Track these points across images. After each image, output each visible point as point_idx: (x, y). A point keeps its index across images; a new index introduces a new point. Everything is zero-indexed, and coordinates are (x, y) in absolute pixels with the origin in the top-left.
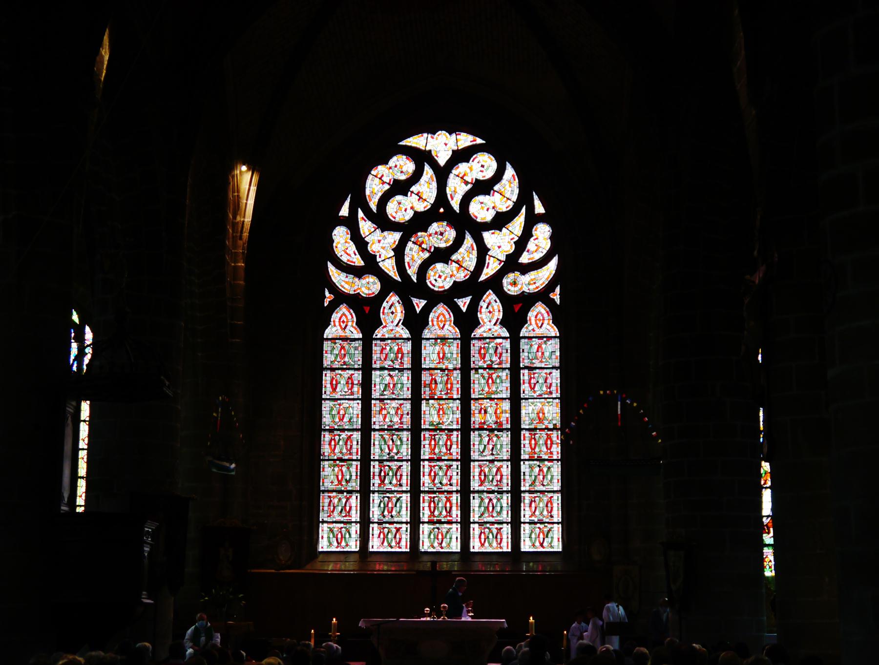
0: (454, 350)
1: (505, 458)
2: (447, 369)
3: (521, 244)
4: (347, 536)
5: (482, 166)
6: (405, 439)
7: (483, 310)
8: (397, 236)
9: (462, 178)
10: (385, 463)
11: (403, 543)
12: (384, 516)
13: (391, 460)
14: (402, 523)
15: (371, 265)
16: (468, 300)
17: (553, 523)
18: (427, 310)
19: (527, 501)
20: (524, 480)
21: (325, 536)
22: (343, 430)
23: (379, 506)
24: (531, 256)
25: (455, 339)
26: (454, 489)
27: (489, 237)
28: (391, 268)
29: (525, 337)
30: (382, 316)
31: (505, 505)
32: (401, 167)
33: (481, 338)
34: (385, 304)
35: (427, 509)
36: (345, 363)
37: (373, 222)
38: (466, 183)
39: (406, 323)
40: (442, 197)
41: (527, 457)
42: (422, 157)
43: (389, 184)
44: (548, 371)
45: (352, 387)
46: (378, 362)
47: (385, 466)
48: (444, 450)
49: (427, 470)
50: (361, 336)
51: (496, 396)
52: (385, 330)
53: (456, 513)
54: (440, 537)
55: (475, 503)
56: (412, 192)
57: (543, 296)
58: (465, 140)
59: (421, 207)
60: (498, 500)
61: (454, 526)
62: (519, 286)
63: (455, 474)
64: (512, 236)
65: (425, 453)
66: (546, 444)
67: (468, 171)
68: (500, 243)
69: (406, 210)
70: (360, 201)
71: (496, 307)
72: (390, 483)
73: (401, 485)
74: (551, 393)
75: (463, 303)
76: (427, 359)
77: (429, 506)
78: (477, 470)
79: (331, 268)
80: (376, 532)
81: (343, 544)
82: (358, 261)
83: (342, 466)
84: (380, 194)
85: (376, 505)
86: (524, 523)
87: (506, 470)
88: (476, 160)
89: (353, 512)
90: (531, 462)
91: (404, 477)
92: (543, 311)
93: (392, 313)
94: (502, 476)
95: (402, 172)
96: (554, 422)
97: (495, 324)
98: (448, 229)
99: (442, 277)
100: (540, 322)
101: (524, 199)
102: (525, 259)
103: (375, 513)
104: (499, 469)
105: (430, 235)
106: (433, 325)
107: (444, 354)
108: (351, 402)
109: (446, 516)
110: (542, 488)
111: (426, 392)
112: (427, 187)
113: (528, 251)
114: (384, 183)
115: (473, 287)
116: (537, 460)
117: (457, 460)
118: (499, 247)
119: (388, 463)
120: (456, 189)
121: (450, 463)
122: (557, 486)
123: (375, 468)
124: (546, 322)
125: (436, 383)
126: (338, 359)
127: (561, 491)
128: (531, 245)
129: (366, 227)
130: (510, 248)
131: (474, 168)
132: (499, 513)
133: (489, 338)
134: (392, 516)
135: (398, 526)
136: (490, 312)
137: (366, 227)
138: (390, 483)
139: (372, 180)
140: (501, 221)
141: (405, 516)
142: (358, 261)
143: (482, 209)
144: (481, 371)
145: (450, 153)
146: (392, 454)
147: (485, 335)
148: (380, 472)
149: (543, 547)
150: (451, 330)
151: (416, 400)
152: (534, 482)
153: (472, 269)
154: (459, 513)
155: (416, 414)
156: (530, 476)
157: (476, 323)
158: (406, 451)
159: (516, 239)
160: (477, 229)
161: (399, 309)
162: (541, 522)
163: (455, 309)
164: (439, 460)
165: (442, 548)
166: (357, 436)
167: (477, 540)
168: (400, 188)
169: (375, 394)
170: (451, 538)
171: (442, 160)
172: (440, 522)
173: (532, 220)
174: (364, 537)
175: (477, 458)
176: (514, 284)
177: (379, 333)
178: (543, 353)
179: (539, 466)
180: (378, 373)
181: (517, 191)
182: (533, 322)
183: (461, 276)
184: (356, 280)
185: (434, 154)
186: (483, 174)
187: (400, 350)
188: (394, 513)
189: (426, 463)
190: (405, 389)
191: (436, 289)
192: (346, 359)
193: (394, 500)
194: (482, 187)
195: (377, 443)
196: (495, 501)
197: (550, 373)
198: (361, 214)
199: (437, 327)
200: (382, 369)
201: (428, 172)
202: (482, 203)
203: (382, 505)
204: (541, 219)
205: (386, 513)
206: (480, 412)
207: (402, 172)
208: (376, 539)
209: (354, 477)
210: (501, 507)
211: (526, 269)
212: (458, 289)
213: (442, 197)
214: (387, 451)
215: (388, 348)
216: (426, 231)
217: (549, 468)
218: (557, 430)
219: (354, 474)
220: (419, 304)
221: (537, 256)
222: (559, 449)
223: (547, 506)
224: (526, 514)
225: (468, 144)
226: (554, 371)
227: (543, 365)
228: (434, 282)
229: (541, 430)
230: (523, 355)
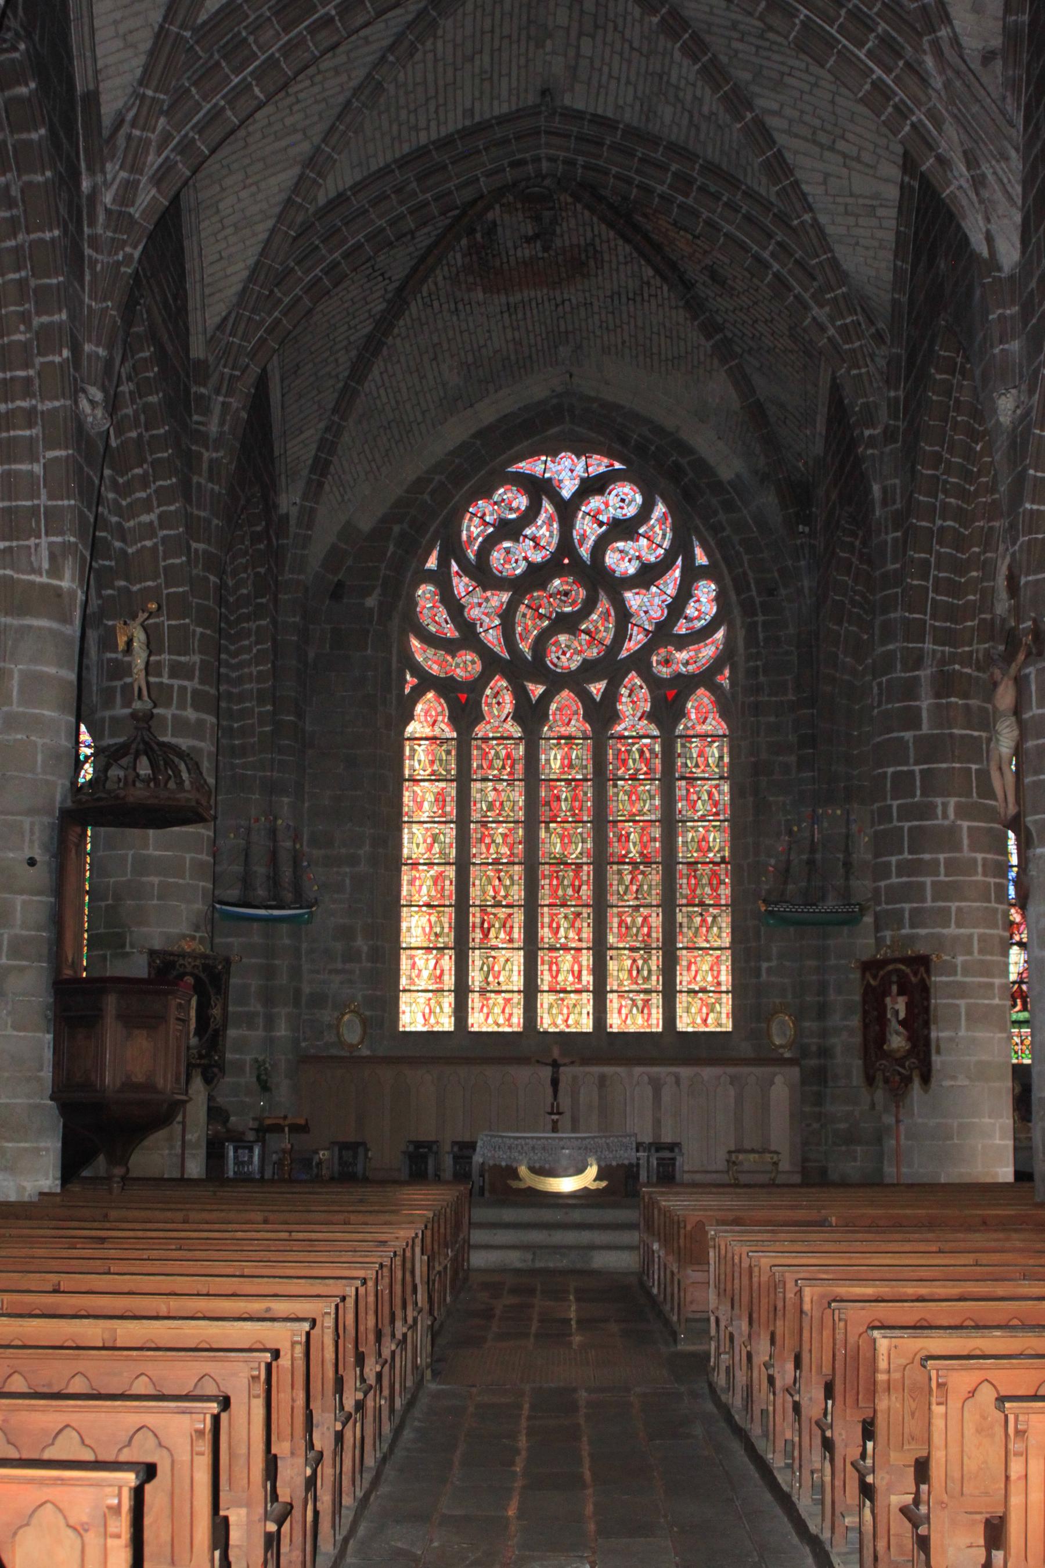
0: (581, 753)
1: (654, 903)
2: (574, 780)
3: (677, 607)
4: (438, 1010)
5: (623, 500)
6: (516, 878)
7: (624, 700)
8: (505, 597)
9: (594, 516)
10: (489, 910)
11: (515, 1020)
12: (488, 984)
14: (512, 992)
15: (468, 636)
16: (602, 685)
17: (721, 992)
18: (546, 698)
19: (684, 963)
20: (681, 932)
22: (431, 864)
23: (482, 969)
24: (691, 625)
25: (585, 738)
26: (584, 945)
27: (633, 599)
28: (495, 642)
29: (681, 737)
30: (485, 708)
31: (654, 968)
32: (510, 503)
33: (621, 737)
34: (488, 692)
35: (546, 973)
37: (471, 579)
38: (601, 524)
39: (518, 716)
40: (566, 544)
41: (684, 901)
42: (539, 489)
43: (493, 525)
45: (444, 806)
47: (488, 914)
48: (570, 892)
49: (546, 920)
50: (455, 735)
52: (488, 727)
53: (587, 978)
54: (565, 1011)
55: (612, 966)
56: (526, 536)
57: (705, 678)
58: (599, 465)
59: (537, 557)
60: (645, 961)
61: (585, 995)
62: (674, 667)
63: (585, 924)
64: (665, 597)
65: (545, 896)
66: (710, 884)
67: (603, 507)
68: (647, 605)
69: (516, 561)
70: (453, 549)
71: (641, 695)
73: (511, 941)
75: (597, 689)
77: (550, 970)
78: (616, 920)
79: (415, 643)
80: (477, 1005)
81: (432, 1021)
82: (450, 631)
84: (480, 539)
85: (477, 968)
86: (681, 992)
87: (656, 921)
88: (614, 493)
89: (446, 977)
90: (690, 909)
91: (516, 930)
92: (706, 700)
93: (499, 703)
94: (650, 928)
95: (511, 509)
98: (575, 587)
99: (567, 654)
100: (702, 715)
101: (680, 547)
102: (681, 628)
103: (475, 978)
104: (645, 919)
105: (551, 596)
106: (555, 721)
107: (570, 760)
108: (442, 826)
109: (573, 984)
111: (544, 813)
112: (545, 530)
113: (686, 618)
114: (486, 524)
115: (610, 666)
117: (588, 906)
118: (646, 612)
119: (493, 910)
120: (587, 529)
121: (579, 909)
122: (727, 941)
123: (475, 917)
124: (711, 716)
125: (559, 799)
128: (691, 611)
129: (461, 585)
130: (658, 613)
131: (611, 503)
132: (647, 979)
135: (507, 996)
136: (633, 702)
137: (461, 585)
139: (471, 520)
140: (648, 575)
141: (518, 982)
142: (450, 631)
143: (621, 559)
144: (620, 783)
145: (577, 482)
147: (626, 734)
148: (483, 921)
149: (706, 1025)
150: (577, 726)
151: (532, 822)
153: (608, 642)
154: (591, 978)
155: (531, 841)
156: (689, 928)
157: (615, 717)
158: (517, 893)
159: (669, 600)
160: (615, 586)
161: (508, 698)
162: (704, 990)
163: (585, 697)
164: (564, 905)
166: (451, 872)
167: (616, 1015)
168: (509, 530)
169: (475, 816)
170: (580, 1014)
171: (566, 493)
173: (691, 575)
174: (461, 1011)
175: (615, 902)
176: (667, 662)
177: (480, 730)
178: (707, 759)
180: (478, 785)
181: (669, 535)
182: (693, 716)
183: (593, 653)
184: (449, 658)
185: (555, 483)
186: (624, 511)
187: (508, 756)
188: (501, 979)
189: (546, 909)
190: (516, 808)
192: (435, 768)
193: (502, 960)
194: (623, 529)
195: (477, 882)
196: (640, 962)
197: (717, 786)
198: (455, 567)
200: (485, 780)
201: (547, 507)
202: (621, 551)
203: (485, 968)
204: (704, 573)
205: (491, 979)
206: (619, 841)
207: (511, 509)
209: (446, 930)
210: (650, 971)
211: (682, 642)
212: (589, 670)
213: (566, 544)
214: (492, 893)
215: (493, 752)
216: (544, 589)
217: (715, 917)
218: (727, 863)
219: (446, 925)
220: (537, 690)
221: (699, 624)
222: (728, 891)
223: (711, 969)
224: (683, 979)
225: (602, 469)
228: (555, 660)
230: (679, 761)
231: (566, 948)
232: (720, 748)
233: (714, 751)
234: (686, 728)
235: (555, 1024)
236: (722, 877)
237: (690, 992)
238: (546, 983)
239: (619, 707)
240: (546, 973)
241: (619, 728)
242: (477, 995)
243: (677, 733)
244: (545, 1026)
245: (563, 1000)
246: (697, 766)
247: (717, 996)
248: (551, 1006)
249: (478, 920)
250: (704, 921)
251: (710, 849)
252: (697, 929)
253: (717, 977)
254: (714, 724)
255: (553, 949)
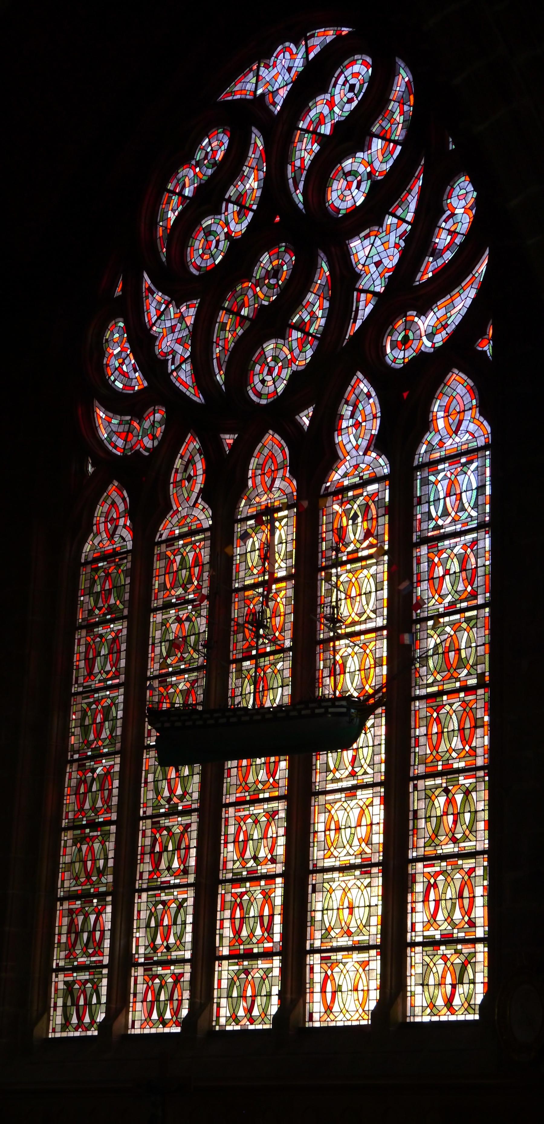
13: (173, 812)
21: (60, 1002)
23: (148, 926)
28: (189, 381)
35: (227, 924)
36: (111, 609)
44: (469, 537)
46: (161, 595)
47: (161, 829)
51: (363, 627)
54: (249, 993)
72: (169, 868)
74: (474, 595)
76: (243, 566)
77: (232, 918)
83: (93, 839)
90: (430, 782)
96: (480, 669)
97: (365, 454)
100: (457, 420)
106: (255, 486)
110: (450, 848)
116: (440, 774)
122: (481, 841)
124: (468, 416)
126: (100, 604)
127: (491, 853)
133: (354, 487)
134: (168, 948)
136: (357, 425)
138: (169, 868)
146: (175, 800)
152: (436, 834)
156: (428, 818)
157: (331, 457)
162: (448, 940)
164: (255, 801)
165: (252, 1021)
167: (317, 997)
172: (249, 955)
179: (447, 791)
188: (172, 940)
191: (264, 402)
195: (150, 778)
197: (475, 542)
199: (260, 489)
200: (167, 606)
208: (139, 1006)
214: (166, 793)
215: (178, 558)
217: (467, 793)
223: (460, 896)
226: (482, 534)
227: (458, 527)
229: (448, 693)
231: (254, 878)
232: (480, 472)
233: (469, 479)
234: (431, 449)
235: (234, 1018)
236: (480, 714)
237: (430, 943)
238: (226, 942)
239: (338, 439)
240: (227, 924)
241: (336, 477)
242: (141, 970)
243: (416, 463)
244: (223, 1021)
245: (247, 972)
246: (446, 513)
247: (466, 950)
248: (232, 983)
249: (148, 841)
250: (450, 801)
251: (461, 663)
252: (440, 818)
253: (469, 912)
254: (475, 431)
255: (238, 881)
